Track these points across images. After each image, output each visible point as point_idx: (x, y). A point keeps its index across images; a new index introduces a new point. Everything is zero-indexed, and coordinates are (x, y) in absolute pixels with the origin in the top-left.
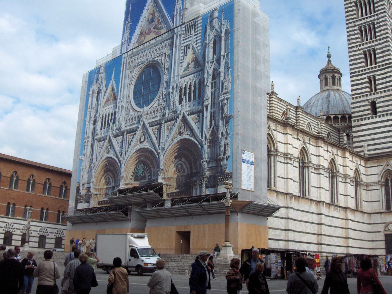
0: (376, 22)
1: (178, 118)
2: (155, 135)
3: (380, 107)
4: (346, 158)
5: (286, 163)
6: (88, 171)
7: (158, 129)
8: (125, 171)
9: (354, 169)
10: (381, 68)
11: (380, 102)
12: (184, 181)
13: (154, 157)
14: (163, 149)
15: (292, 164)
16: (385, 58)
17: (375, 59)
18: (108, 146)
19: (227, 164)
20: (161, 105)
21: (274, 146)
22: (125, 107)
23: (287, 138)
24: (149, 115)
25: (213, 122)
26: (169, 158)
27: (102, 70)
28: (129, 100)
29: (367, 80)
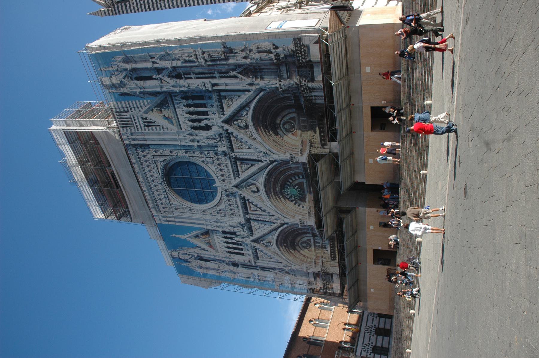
1: (227, 130)
2: (249, 168)
6: (293, 276)
7: (242, 163)
8: (294, 217)
12: (305, 119)
13: (275, 169)
14: (266, 153)
18: (263, 244)
19: (283, 48)
20: (214, 159)
22: (216, 217)
24: (226, 178)
25: (231, 73)
26: (277, 145)
27: (175, 254)
28: (208, 210)
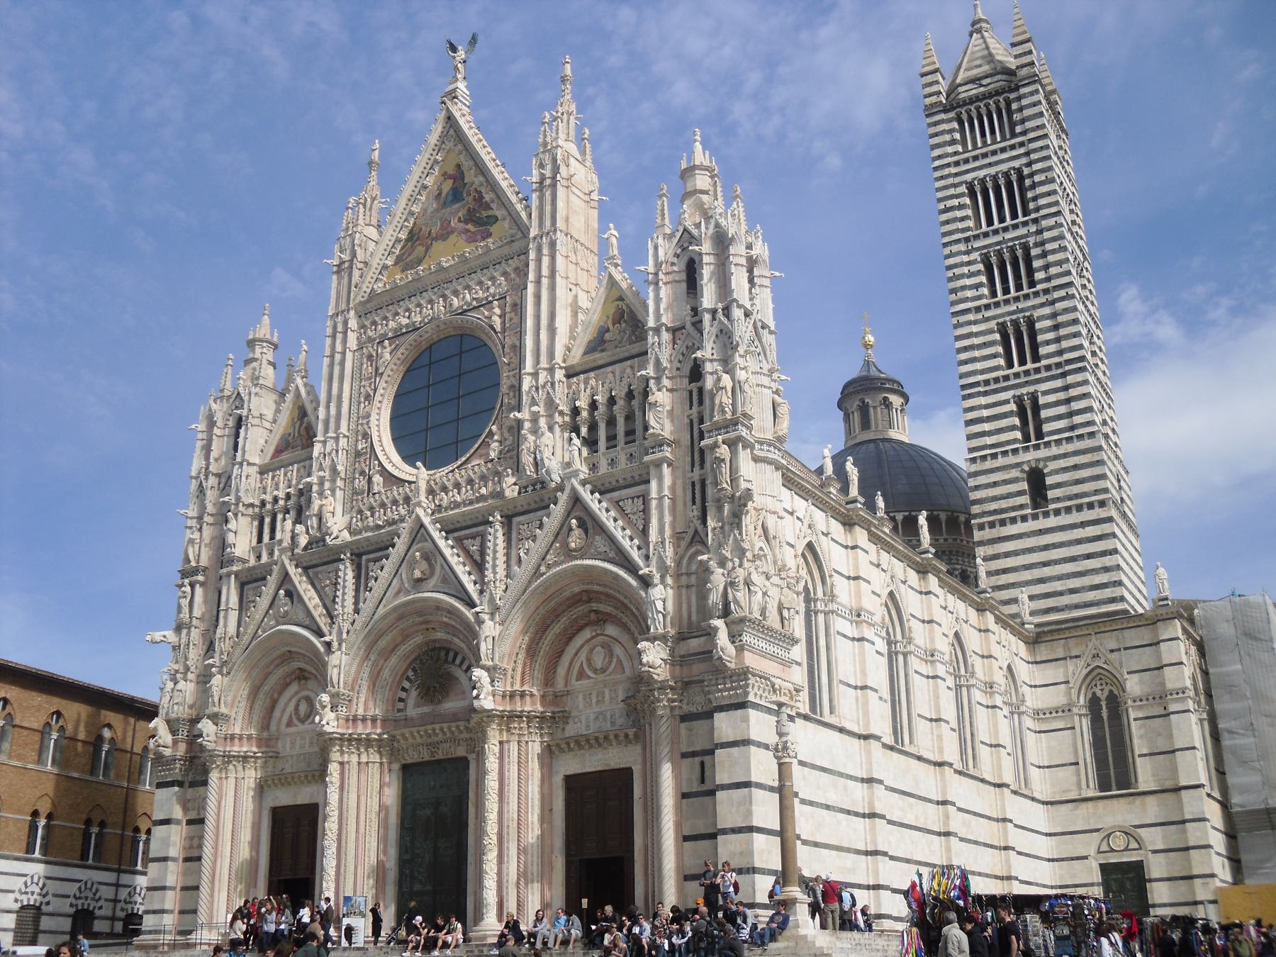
0: (1031, 240)
3: (1059, 485)
4: (987, 631)
5: (859, 640)
9: (1005, 668)
10: (1055, 372)
11: (1057, 472)
15: (873, 643)
16: (1065, 344)
17: (1035, 347)
21: (824, 582)
23: (856, 559)
29: (1013, 407)
